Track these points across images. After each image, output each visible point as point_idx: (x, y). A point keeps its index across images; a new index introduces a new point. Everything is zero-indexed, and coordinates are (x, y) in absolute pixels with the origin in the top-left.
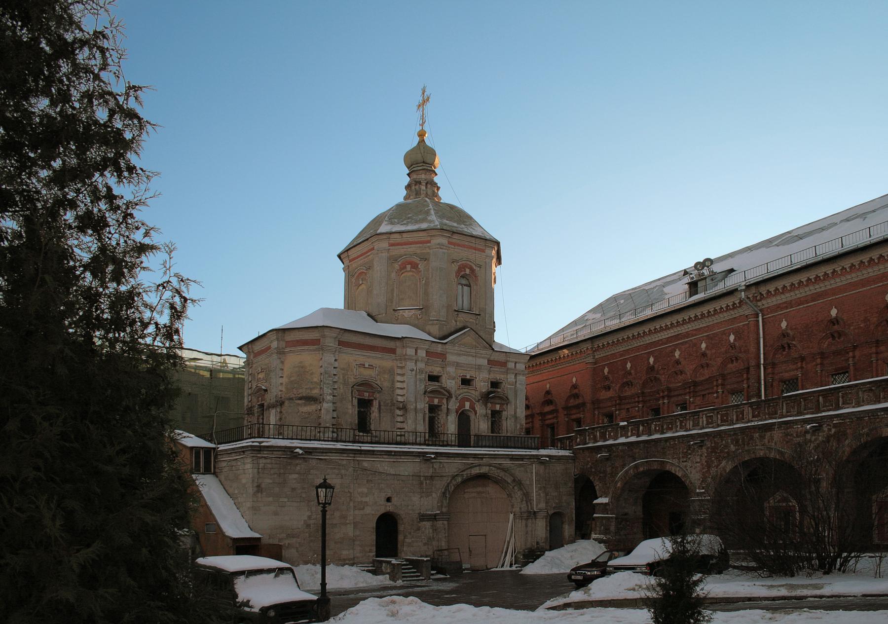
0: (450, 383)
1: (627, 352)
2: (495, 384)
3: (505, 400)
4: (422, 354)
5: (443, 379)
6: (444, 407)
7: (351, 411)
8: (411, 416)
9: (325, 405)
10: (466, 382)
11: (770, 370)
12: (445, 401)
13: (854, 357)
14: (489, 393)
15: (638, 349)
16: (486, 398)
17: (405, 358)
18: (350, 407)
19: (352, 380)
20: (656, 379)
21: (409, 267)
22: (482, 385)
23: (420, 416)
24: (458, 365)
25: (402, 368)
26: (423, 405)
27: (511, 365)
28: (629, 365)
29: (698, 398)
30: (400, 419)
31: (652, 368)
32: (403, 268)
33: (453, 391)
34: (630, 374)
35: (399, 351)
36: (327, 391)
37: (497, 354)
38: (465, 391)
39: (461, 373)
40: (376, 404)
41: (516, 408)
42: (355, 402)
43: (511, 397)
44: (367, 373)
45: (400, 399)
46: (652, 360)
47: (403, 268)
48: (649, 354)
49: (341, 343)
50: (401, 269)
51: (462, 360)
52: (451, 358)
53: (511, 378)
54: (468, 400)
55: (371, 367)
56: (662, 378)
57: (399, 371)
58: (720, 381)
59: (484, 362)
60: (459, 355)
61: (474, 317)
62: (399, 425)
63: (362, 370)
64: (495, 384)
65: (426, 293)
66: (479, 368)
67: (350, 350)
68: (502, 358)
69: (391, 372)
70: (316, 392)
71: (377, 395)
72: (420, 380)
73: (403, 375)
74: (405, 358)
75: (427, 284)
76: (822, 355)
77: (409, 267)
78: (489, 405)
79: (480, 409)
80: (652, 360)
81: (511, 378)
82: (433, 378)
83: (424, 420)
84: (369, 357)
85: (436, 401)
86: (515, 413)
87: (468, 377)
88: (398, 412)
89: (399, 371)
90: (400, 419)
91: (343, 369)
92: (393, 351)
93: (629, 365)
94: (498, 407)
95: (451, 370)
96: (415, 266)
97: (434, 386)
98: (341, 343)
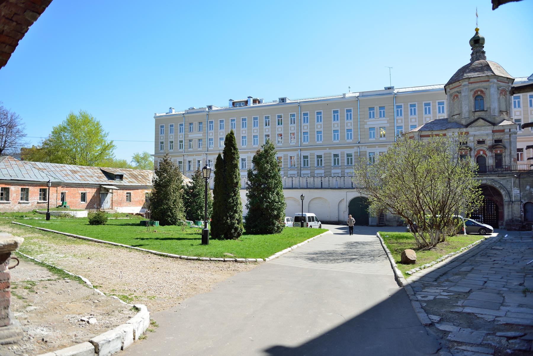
16: (492, 148)
22: (489, 142)
33: (473, 148)
39: (477, 138)
43: (507, 145)
51: (477, 133)
60: (476, 131)
65: (461, 107)
66: (487, 135)
78: (494, 151)
79: (489, 153)
86: (511, 153)
87: (481, 140)
94: (499, 152)
95: (471, 138)
96: (457, 96)
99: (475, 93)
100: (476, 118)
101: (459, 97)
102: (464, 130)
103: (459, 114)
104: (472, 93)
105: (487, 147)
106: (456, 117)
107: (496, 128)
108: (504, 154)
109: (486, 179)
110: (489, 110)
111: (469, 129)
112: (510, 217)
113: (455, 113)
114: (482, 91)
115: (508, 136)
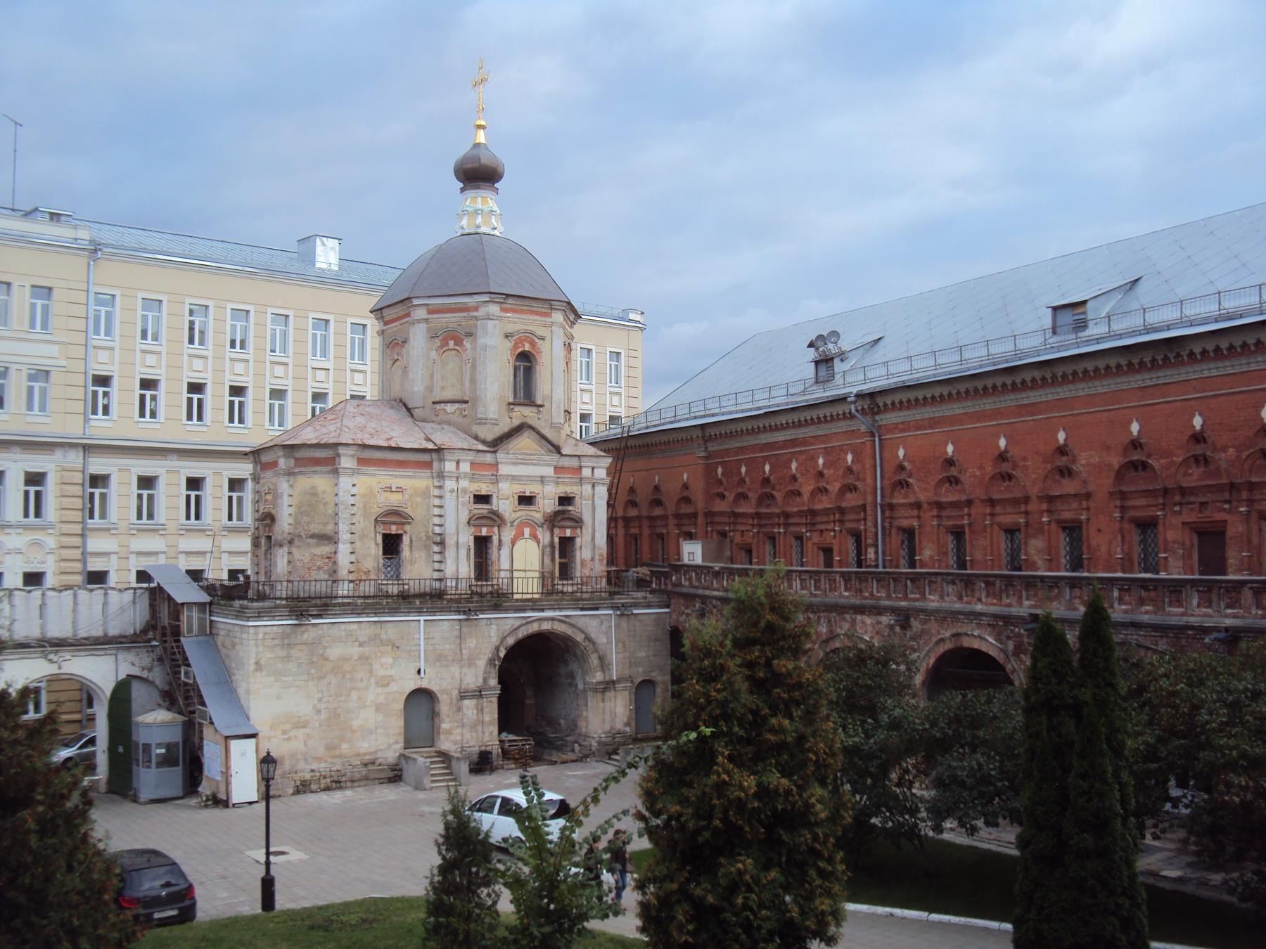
0: (505, 505)
1: (742, 450)
2: (565, 500)
3: (577, 522)
4: (465, 467)
5: (494, 500)
6: (495, 539)
7: (374, 549)
8: (450, 553)
9: (341, 547)
10: (526, 500)
11: (887, 514)
12: (496, 529)
13: (969, 515)
14: (556, 514)
15: (753, 448)
16: (553, 520)
17: (441, 475)
18: (373, 546)
19: (376, 511)
20: (773, 497)
21: (451, 343)
22: (547, 503)
23: (463, 552)
24: (513, 478)
25: (440, 487)
26: (467, 539)
27: (586, 472)
28: (743, 469)
29: (815, 534)
30: (437, 557)
31: (766, 481)
32: (445, 343)
34: (745, 482)
35: (436, 465)
36: (343, 528)
37: (567, 459)
38: (525, 512)
39: (518, 489)
40: (406, 539)
41: (594, 531)
42: (380, 539)
43: (587, 517)
44: (394, 500)
45: (437, 530)
46: (767, 468)
47: (445, 343)
48: (766, 458)
49: (362, 461)
50: (442, 346)
52: (504, 470)
53: (587, 489)
54: (527, 525)
55: (400, 490)
56: (779, 495)
57: (437, 492)
58: (837, 516)
59: (550, 471)
61: (534, 409)
62: (437, 566)
63: (388, 494)
64: (565, 500)
65: (473, 381)
66: (542, 480)
67: (372, 469)
68: (574, 463)
69: (425, 494)
70: (329, 529)
71: (407, 528)
72: (463, 504)
73: (441, 497)
74: (441, 475)
75: (474, 367)
76: (940, 506)
77: (451, 343)
78: (557, 531)
80: (767, 468)
81: (587, 489)
82: (482, 499)
83: (468, 559)
84: (396, 476)
85: (484, 532)
86: (593, 538)
87: (528, 494)
88: (436, 549)
89: (437, 492)
90: (437, 557)
91: (364, 496)
92: (429, 465)
93: (743, 469)
94: (568, 533)
95: (505, 487)
96: (459, 342)
97: (483, 509)
98: (362, 461)
99: (516, 347)
100: (516, 422)
101: (467, 344)
102: (489, 458)
103: (466, 402)
104: (509, 345)
105: (538, 517)
106: (450, 408)
107: (566, 462)
108: (578, 540)
109: (553, 619)
110: (547, 404)
111: (501, 456)
112: (607, 727)
113: (449, 394)
114: (533, 344)
115: (589, 487)
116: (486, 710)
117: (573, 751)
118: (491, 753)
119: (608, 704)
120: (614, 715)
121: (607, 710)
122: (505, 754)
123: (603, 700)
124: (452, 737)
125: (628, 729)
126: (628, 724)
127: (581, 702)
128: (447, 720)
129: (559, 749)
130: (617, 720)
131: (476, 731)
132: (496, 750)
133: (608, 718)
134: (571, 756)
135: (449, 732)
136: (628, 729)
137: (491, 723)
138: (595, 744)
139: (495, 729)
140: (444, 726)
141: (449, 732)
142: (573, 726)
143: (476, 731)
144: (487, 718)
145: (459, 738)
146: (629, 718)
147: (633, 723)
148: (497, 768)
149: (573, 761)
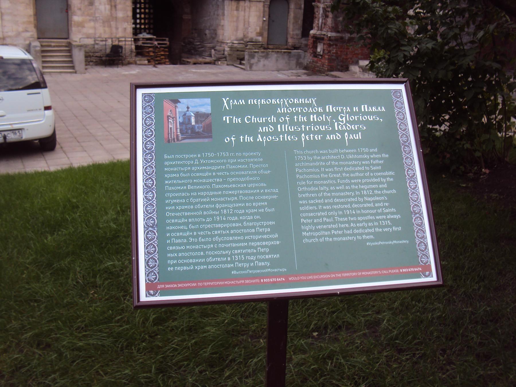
112: (240, 35)
116: (119, 7)
117: (210, 56)
118: (121, 47)
119: (242, 13)
120: (247, 23)
121: (241, 18)
122: (140, 51)
123: (237, 9)
124: (85, 30)
125: (260, 39)
126: (260, 34)
127: (220, 12)
128: (79, 12)
129: (200, 54)
130: (250, 30)
131: (110, 26)
132: (129, 45)
133: (241, 26)
134: (208, 59)
135: (81, 25)
136: (260, 39)
137: (124, 20)
138: (227, 49)
139: (129, 27)
140: (76, 18)
141: (81, 25)
142: (215, 33)
143: (110, 26)
144: (120, 14)
145: (91, 31)
146: (262, 28)
147: (266, 34)
148: (129, 63)
149: (206, 63)
